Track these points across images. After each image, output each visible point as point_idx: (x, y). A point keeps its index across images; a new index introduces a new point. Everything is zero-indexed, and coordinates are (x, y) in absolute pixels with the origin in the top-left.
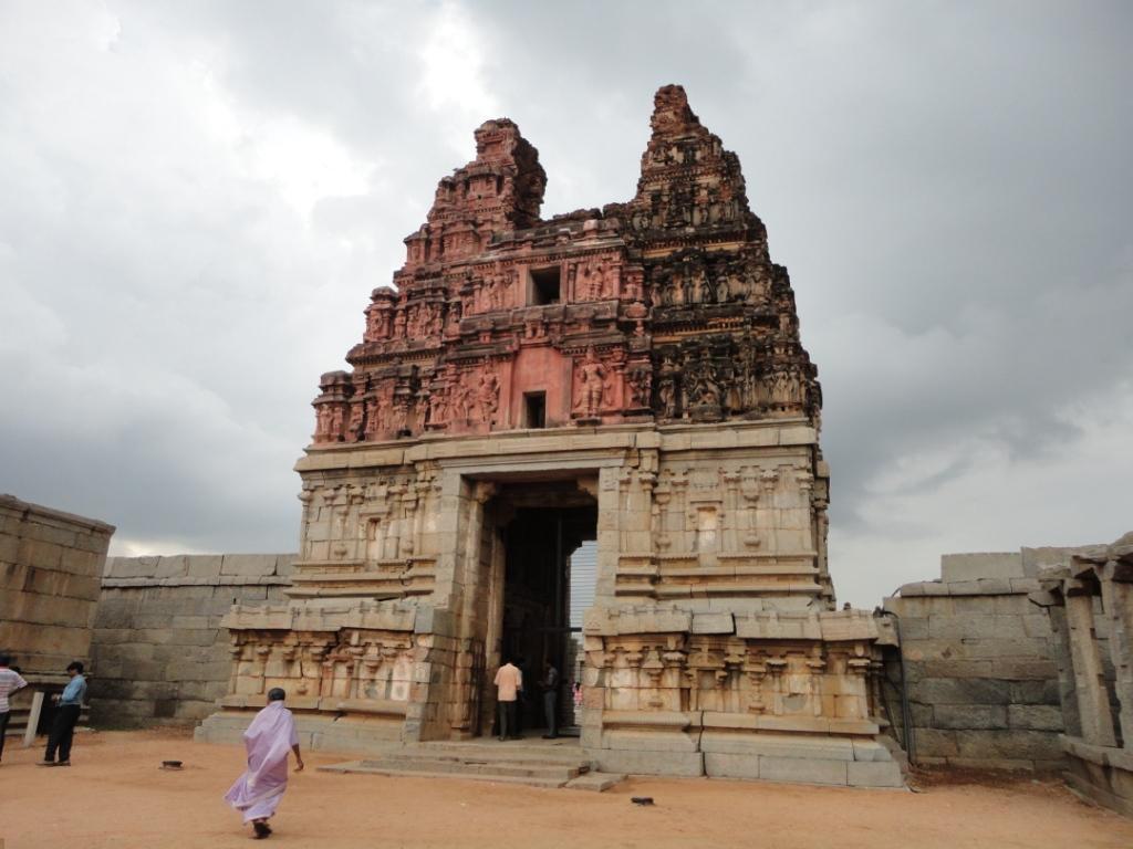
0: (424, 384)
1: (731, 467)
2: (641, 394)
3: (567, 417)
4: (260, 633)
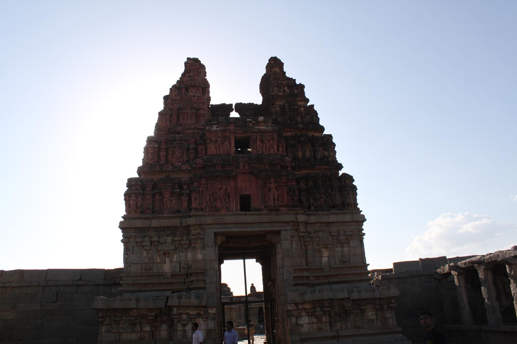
0: (184, 187)
2: (295, 198)
3: (263, 207)
4: (115, 310)
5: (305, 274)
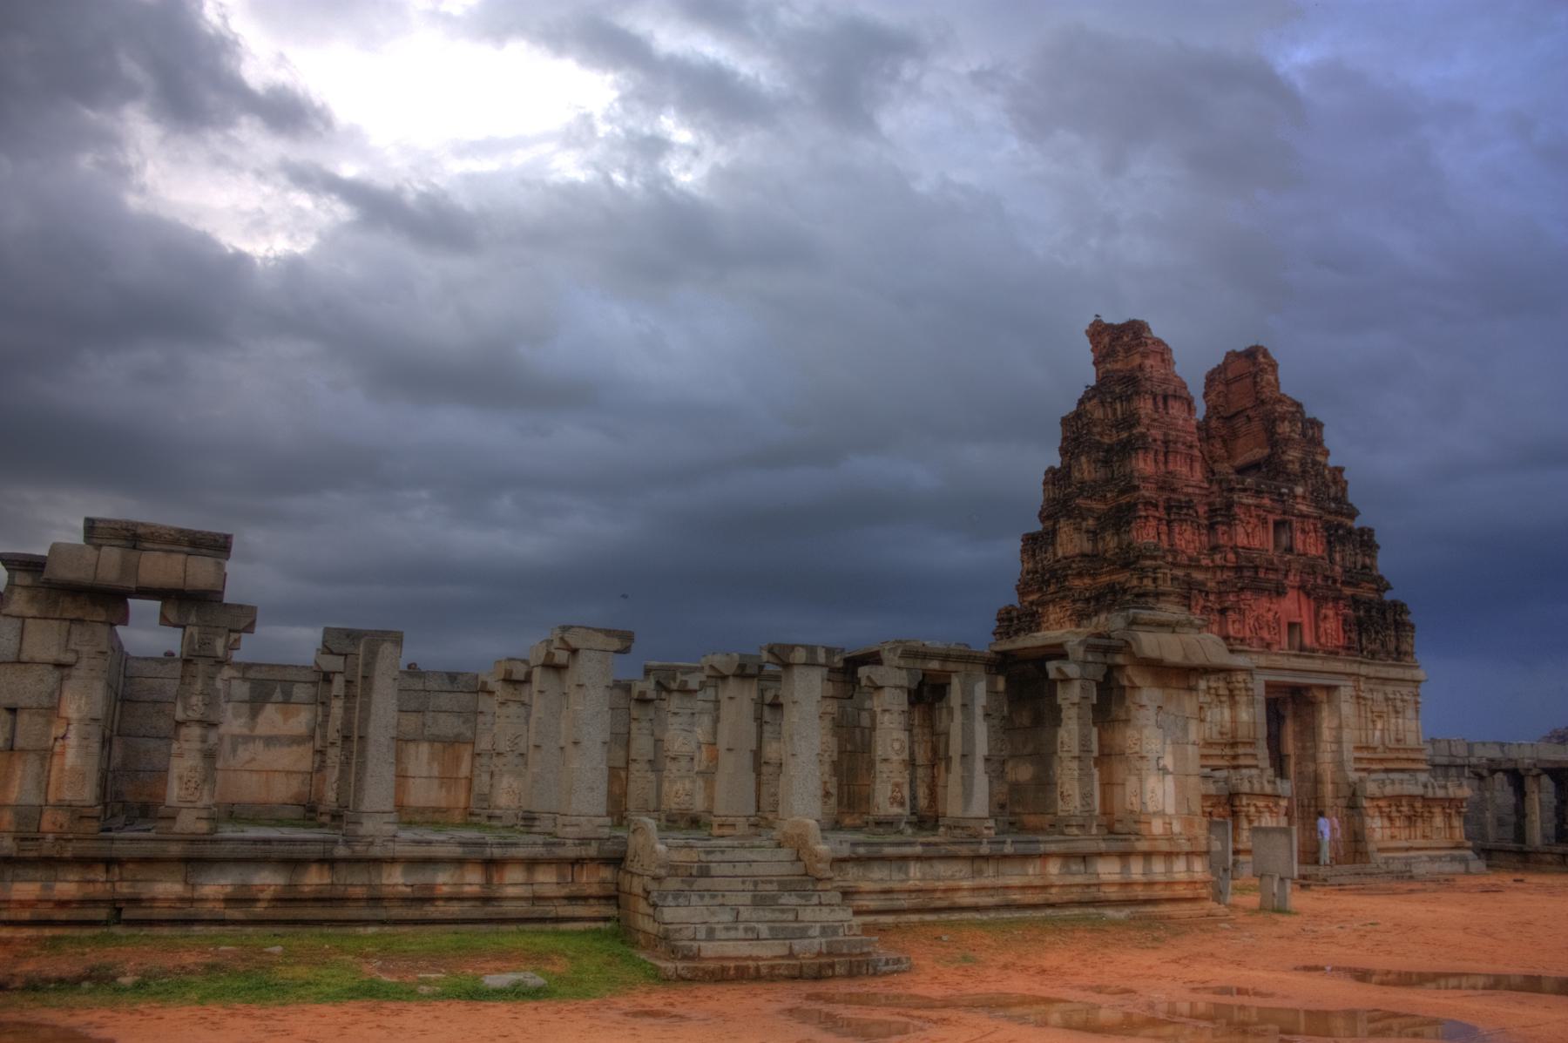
1: (1389, 689)
5: (1365, 754)
